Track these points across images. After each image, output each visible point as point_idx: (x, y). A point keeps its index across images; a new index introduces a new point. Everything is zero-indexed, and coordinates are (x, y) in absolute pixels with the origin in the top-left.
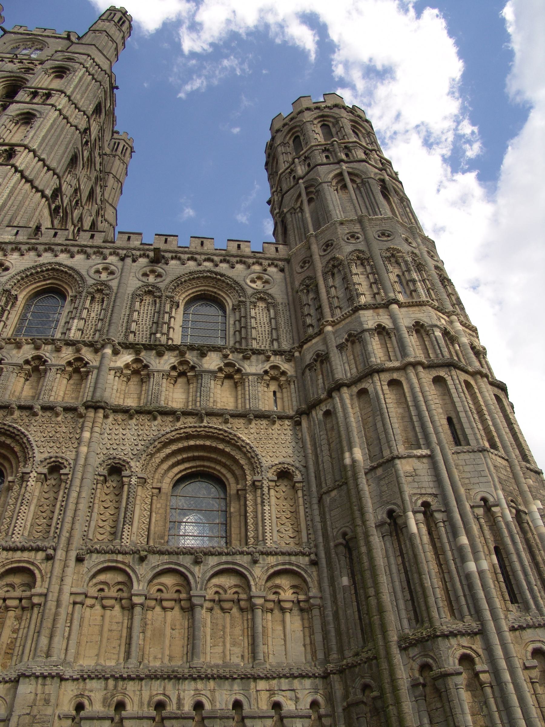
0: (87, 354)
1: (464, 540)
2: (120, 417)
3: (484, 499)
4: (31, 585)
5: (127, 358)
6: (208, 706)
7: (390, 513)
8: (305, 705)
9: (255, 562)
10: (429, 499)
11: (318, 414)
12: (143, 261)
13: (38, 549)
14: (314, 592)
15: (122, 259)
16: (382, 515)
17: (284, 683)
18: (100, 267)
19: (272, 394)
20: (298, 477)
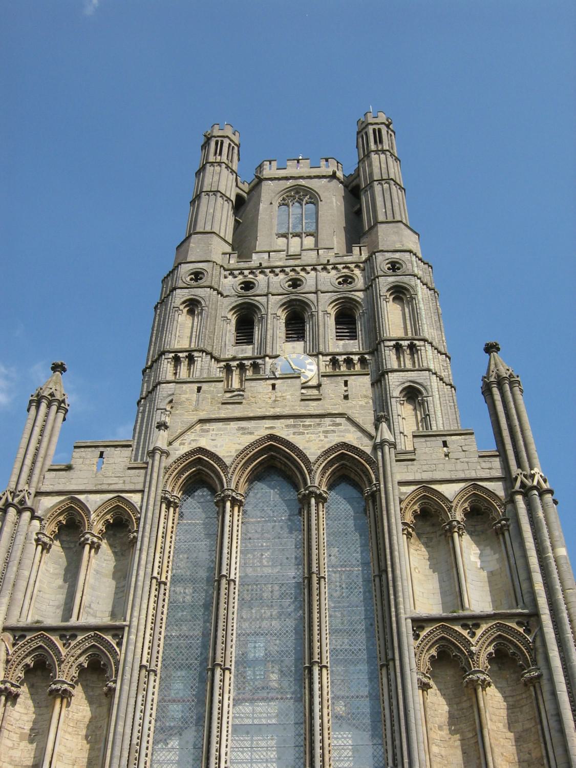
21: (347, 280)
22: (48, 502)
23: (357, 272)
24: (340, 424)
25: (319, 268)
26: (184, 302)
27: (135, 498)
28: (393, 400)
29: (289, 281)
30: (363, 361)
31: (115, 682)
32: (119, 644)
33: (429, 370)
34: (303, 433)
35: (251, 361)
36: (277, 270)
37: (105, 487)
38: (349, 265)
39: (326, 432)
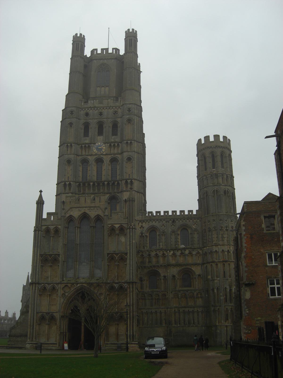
0: (165, 253)
1: (221, 294)
2: (173, 266)
3: (226, 288)
4: (166, 296)
5: (172, 252)
6: (189, 311)
7: (213, 288)
8: (201, 310)
9: (195, 291)
10: (218, 287)
11: (205, 265)
12: (170, 222)
13: (166, 291)
14: (203, 295)
15: (166, 222)
16: (212, 288)
17: (199, 308)
18: (162, 225)
19: (198, 257)
20: (202, 276)
21: (115, 113)
22: (44, 228)
23: (119, 110)
24: (98, 209)
25: (108, 108)
26: (69, 123)
27: (60, 227)
28: (124, 162)
29: (100, 112)
30: (118, 145)
31: (59, 264)
32: (59, 257)
33: (135, 152)
34: (91, 211)
35: (88, 145)
36: (96, 109)
37: (53, 224)
38: (117, 107)
39: (95, 211)
